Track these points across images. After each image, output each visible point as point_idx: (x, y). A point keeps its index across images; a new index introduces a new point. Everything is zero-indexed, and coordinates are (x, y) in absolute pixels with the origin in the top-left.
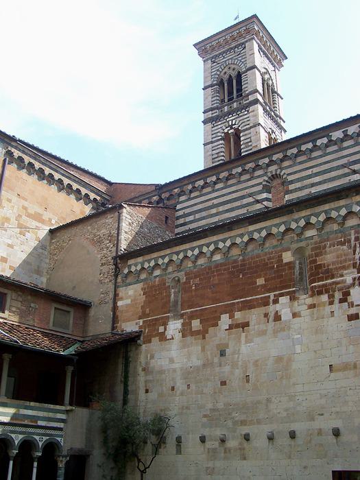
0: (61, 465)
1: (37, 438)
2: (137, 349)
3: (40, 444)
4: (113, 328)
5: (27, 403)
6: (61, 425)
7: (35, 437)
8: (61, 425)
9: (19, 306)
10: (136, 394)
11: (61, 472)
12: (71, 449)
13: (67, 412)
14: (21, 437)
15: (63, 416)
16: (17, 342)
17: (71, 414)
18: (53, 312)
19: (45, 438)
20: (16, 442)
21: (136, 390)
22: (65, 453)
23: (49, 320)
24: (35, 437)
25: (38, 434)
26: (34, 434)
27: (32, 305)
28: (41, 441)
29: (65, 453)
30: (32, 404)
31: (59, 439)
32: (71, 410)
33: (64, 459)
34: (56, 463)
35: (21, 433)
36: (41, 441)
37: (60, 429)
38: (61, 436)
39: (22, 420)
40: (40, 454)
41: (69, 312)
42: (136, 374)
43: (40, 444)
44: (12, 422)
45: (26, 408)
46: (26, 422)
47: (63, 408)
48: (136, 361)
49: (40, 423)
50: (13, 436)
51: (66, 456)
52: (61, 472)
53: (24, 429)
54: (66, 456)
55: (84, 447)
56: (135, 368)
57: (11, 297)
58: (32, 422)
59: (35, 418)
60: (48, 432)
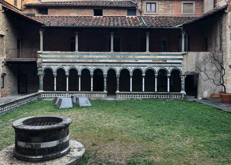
0: (183, 79)
1: (167, 68)
2: (226, 16)
3: (169, 71)
4: (214, 6)
5: (160, 53)
6: (180, 61)
7: (166, 67)
8: (180, 61)
9: (163, 7)
10: (226, 41)
11: (183, 82)
12: (187, 72)
13: (183, 55)
14: (158, 68)
15: (182, 57)
16: (147, 27)
17: (185, 56)
18: (182, 4)
19: (171, 68)
20: (157, 71)
21: (226, 39)
22: (183, 74)
23: (181, 10)
24: (166, 67)
25: (167, 66)
26: (166, 66)
27: (170, 5)
28: (169, 69)
29: (183, 74)
30: (163, 53)
31: (179, 68)
32: (186, 54)
33: (183, 77)
34: (180, 78)
35: (158, 66)
36: (169, 69)
37: (180, 63)
38: (181, 66)
39: (158, 61)
40: (170, 75)
41: (192, 3)
42: (226, 30)
43: (169, 71)
44: (153, 62)
45: (159, 55)
46: (160, 62)
47: (180, 53)
48: (226, 23)
49: (168, 61)
50: (155, 68)
51: (184, 76)
52: (183, 82)
53: (160, 65)
54: (184, 76)
55: (194, 70)
56: (225, 26)
57: (158, 4)
58: (163, 61)
59: (165, 60)
60: (173, 65)
